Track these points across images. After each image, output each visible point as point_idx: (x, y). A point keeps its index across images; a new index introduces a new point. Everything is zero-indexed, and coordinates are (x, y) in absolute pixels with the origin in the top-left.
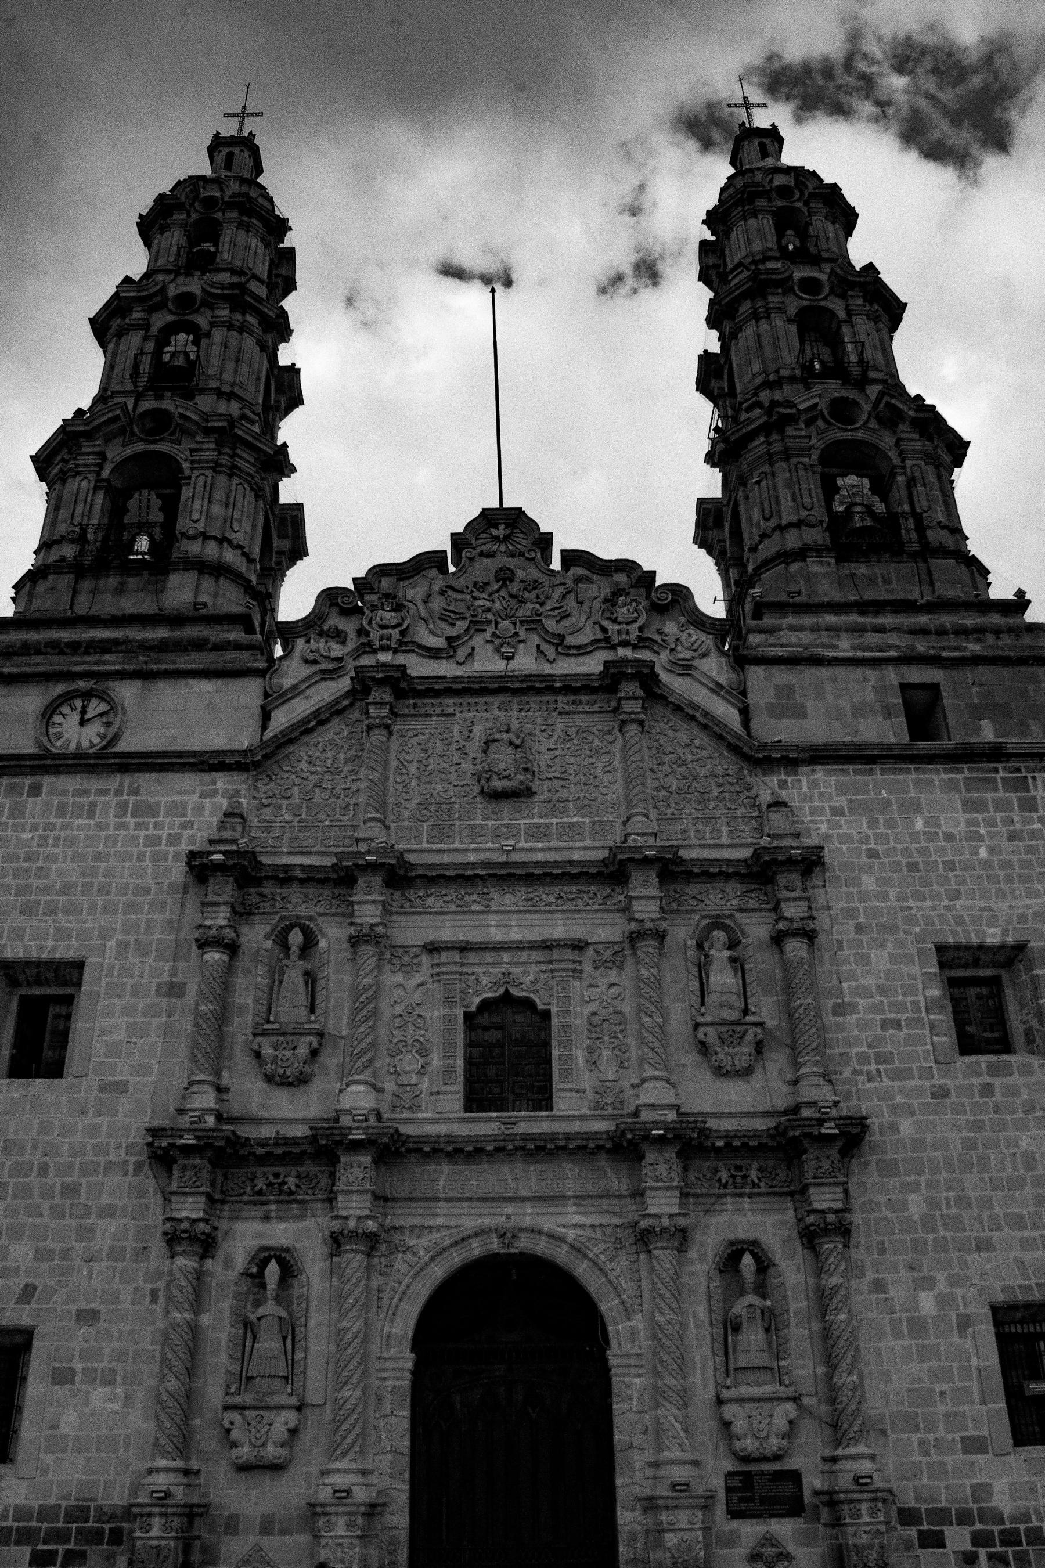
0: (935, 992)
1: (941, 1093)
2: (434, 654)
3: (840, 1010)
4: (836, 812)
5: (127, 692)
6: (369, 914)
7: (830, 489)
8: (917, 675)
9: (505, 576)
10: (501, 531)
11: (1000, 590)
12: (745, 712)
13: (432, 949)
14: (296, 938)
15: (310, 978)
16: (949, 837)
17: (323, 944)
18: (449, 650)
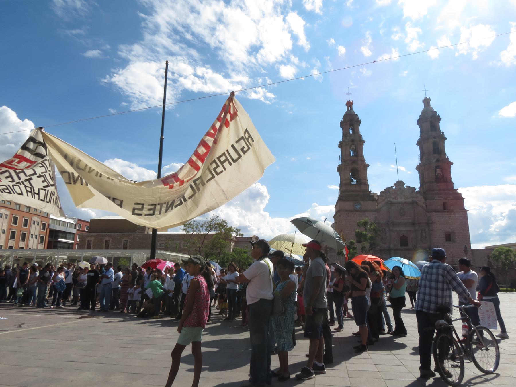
0: (444, 236)
1: (444, 246)
2: (394, 199)
3: (435, 237)
4: (435, 217)
5: (362, 202)
6: (391, 228)
7: (436, 171)
8: (445, 201)
9: (400, 189)
10: (400, 183)
11: (455, 188)
12: (426, 206)
13: (397, 231)
14: (384, 230)
15: (386, 234)
16: (447, 220)
17: (386, 230)
18: (395, 198)
